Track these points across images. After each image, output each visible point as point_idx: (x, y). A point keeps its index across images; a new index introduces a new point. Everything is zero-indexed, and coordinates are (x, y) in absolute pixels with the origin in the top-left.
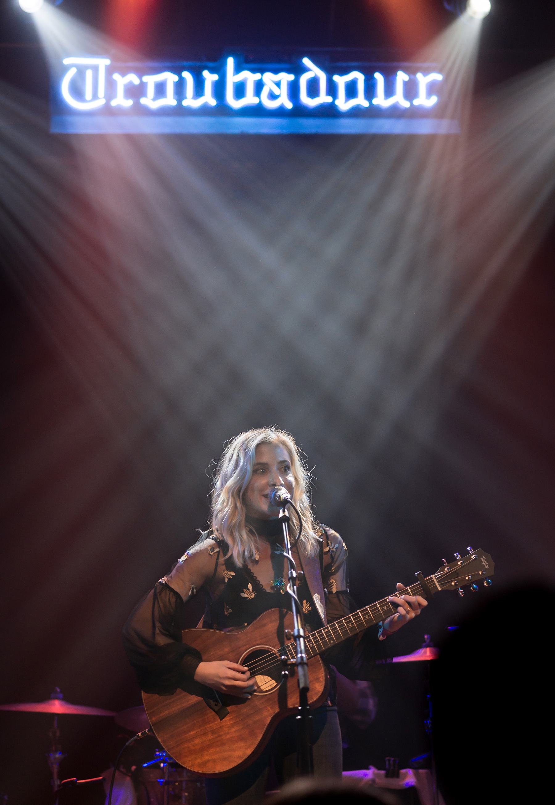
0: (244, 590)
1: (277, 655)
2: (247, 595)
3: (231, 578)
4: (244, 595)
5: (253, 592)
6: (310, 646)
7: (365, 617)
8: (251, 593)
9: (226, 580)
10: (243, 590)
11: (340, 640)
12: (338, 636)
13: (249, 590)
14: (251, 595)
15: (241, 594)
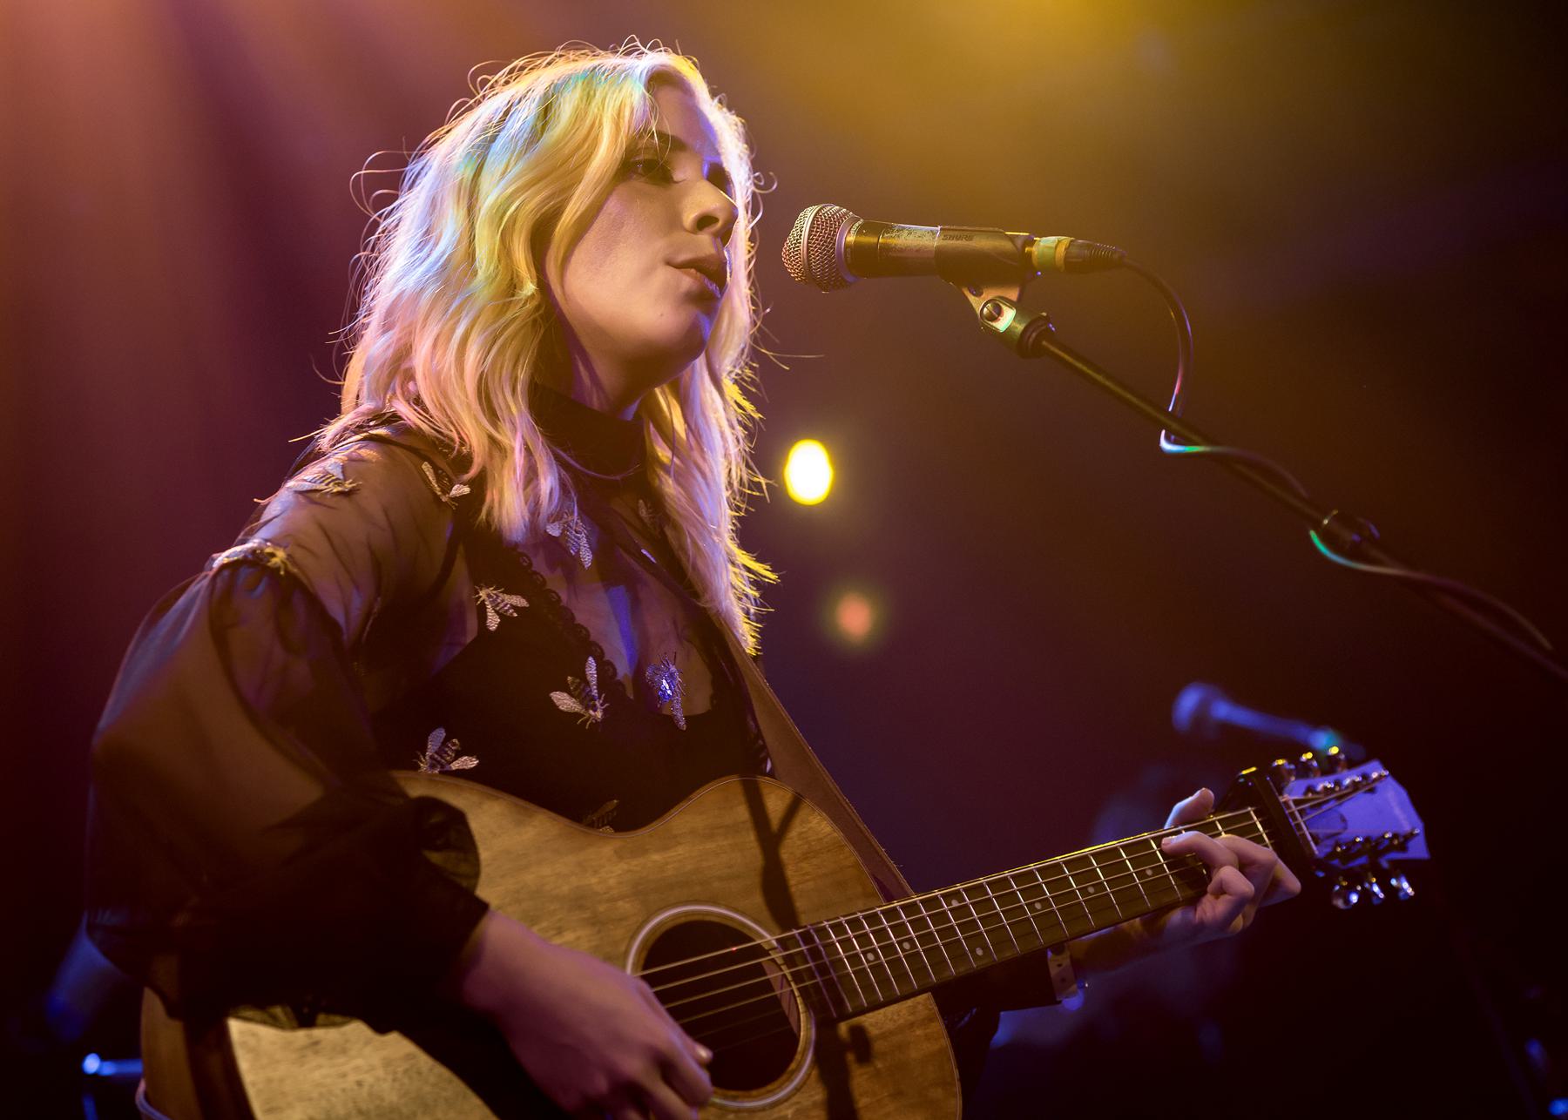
0: (569, 678)
1: (774, 955)
2: (581, 703)
3: (515, 615)
4: (564, 701)
5: (600, 698)
6: (903, 950)
7: (1144, 870)
8: (593, 699)
9: (493, 622)
10: (567, 677)
11: (1008, 954)
12: (998, 933)
13: (587, 683)
14: (595, 711)
15: (552, 694)
